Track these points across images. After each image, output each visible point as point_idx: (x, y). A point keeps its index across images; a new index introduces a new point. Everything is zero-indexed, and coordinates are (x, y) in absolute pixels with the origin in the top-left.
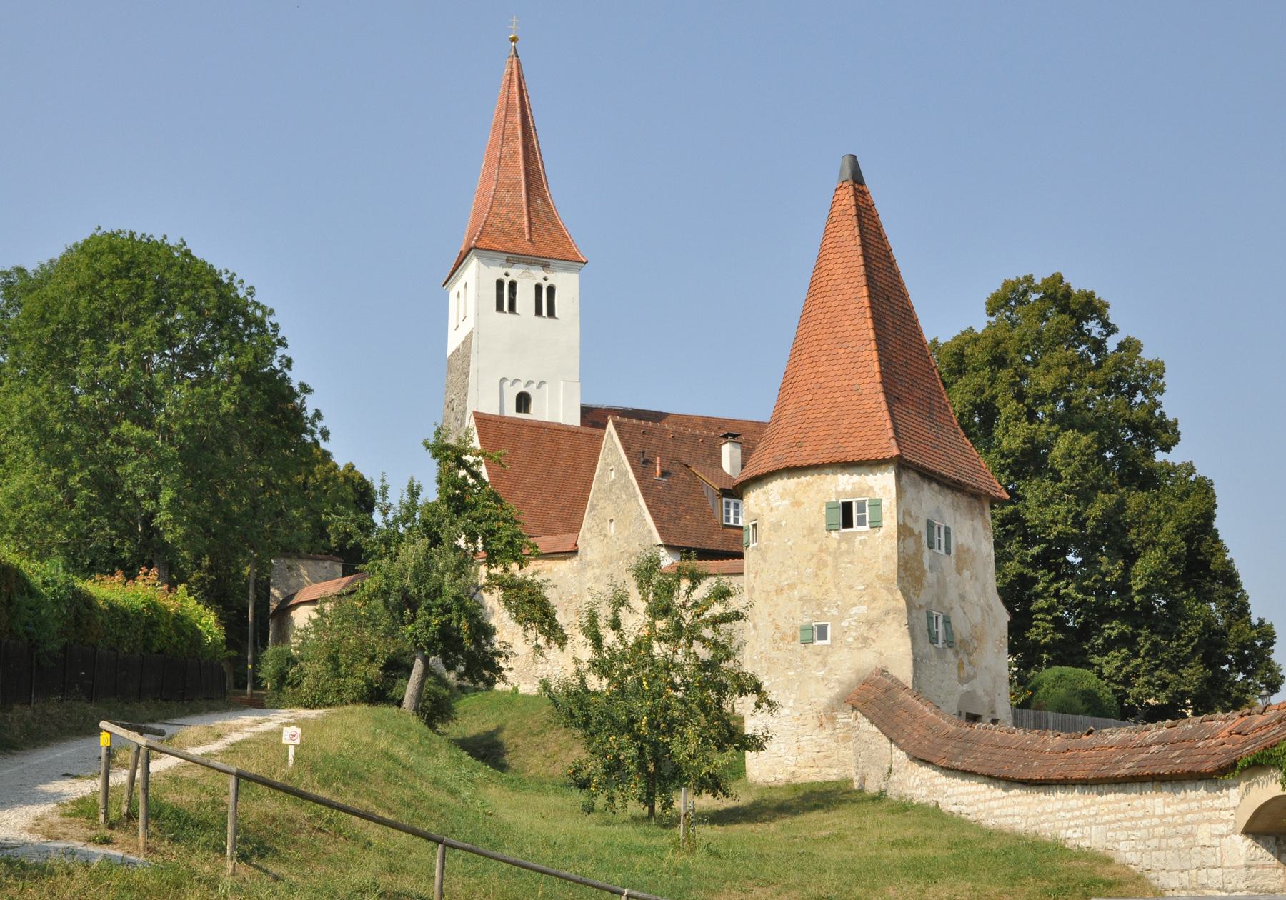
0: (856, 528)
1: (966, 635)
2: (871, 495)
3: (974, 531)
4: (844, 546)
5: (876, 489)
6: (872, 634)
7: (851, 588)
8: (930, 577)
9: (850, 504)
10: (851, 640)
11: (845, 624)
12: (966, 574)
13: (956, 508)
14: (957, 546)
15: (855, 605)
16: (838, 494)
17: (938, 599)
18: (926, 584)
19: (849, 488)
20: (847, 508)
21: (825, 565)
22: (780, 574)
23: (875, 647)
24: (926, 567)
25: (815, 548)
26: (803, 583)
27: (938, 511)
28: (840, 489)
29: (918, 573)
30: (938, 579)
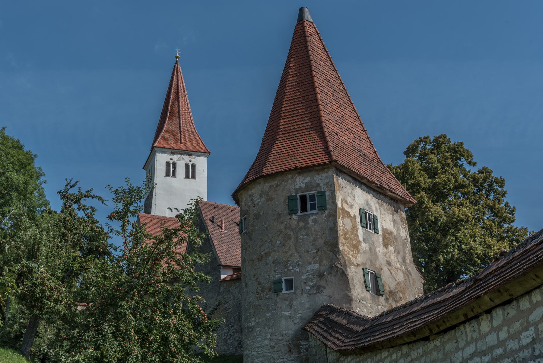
0: (310, 212)
1: (392, 288)
2: (318, 189)
3: (394, 222)
4: (301, 224)
5: (322, 185)
6: (322, 283)
7: (307, 252)
8: (364, 246)
9: (305, 196)
10: (308, 288)
11: (304, 277)
12: (391, 248)
13: (381, 205)
14: (383, 230)
15: (310, 263)
16: (297, 190)
17: (371, 261)
18: (361, 250)
19: (303, 186)
20: (303, 198)
21: (290, 238)
22: (260, 247)
23: (325, 292)
24: (361, 239)
25: (282, 226)
26: (275, 251)
27: (367, 203)
28: (298, 187)
29: (354, 242)
30: (370, 248)
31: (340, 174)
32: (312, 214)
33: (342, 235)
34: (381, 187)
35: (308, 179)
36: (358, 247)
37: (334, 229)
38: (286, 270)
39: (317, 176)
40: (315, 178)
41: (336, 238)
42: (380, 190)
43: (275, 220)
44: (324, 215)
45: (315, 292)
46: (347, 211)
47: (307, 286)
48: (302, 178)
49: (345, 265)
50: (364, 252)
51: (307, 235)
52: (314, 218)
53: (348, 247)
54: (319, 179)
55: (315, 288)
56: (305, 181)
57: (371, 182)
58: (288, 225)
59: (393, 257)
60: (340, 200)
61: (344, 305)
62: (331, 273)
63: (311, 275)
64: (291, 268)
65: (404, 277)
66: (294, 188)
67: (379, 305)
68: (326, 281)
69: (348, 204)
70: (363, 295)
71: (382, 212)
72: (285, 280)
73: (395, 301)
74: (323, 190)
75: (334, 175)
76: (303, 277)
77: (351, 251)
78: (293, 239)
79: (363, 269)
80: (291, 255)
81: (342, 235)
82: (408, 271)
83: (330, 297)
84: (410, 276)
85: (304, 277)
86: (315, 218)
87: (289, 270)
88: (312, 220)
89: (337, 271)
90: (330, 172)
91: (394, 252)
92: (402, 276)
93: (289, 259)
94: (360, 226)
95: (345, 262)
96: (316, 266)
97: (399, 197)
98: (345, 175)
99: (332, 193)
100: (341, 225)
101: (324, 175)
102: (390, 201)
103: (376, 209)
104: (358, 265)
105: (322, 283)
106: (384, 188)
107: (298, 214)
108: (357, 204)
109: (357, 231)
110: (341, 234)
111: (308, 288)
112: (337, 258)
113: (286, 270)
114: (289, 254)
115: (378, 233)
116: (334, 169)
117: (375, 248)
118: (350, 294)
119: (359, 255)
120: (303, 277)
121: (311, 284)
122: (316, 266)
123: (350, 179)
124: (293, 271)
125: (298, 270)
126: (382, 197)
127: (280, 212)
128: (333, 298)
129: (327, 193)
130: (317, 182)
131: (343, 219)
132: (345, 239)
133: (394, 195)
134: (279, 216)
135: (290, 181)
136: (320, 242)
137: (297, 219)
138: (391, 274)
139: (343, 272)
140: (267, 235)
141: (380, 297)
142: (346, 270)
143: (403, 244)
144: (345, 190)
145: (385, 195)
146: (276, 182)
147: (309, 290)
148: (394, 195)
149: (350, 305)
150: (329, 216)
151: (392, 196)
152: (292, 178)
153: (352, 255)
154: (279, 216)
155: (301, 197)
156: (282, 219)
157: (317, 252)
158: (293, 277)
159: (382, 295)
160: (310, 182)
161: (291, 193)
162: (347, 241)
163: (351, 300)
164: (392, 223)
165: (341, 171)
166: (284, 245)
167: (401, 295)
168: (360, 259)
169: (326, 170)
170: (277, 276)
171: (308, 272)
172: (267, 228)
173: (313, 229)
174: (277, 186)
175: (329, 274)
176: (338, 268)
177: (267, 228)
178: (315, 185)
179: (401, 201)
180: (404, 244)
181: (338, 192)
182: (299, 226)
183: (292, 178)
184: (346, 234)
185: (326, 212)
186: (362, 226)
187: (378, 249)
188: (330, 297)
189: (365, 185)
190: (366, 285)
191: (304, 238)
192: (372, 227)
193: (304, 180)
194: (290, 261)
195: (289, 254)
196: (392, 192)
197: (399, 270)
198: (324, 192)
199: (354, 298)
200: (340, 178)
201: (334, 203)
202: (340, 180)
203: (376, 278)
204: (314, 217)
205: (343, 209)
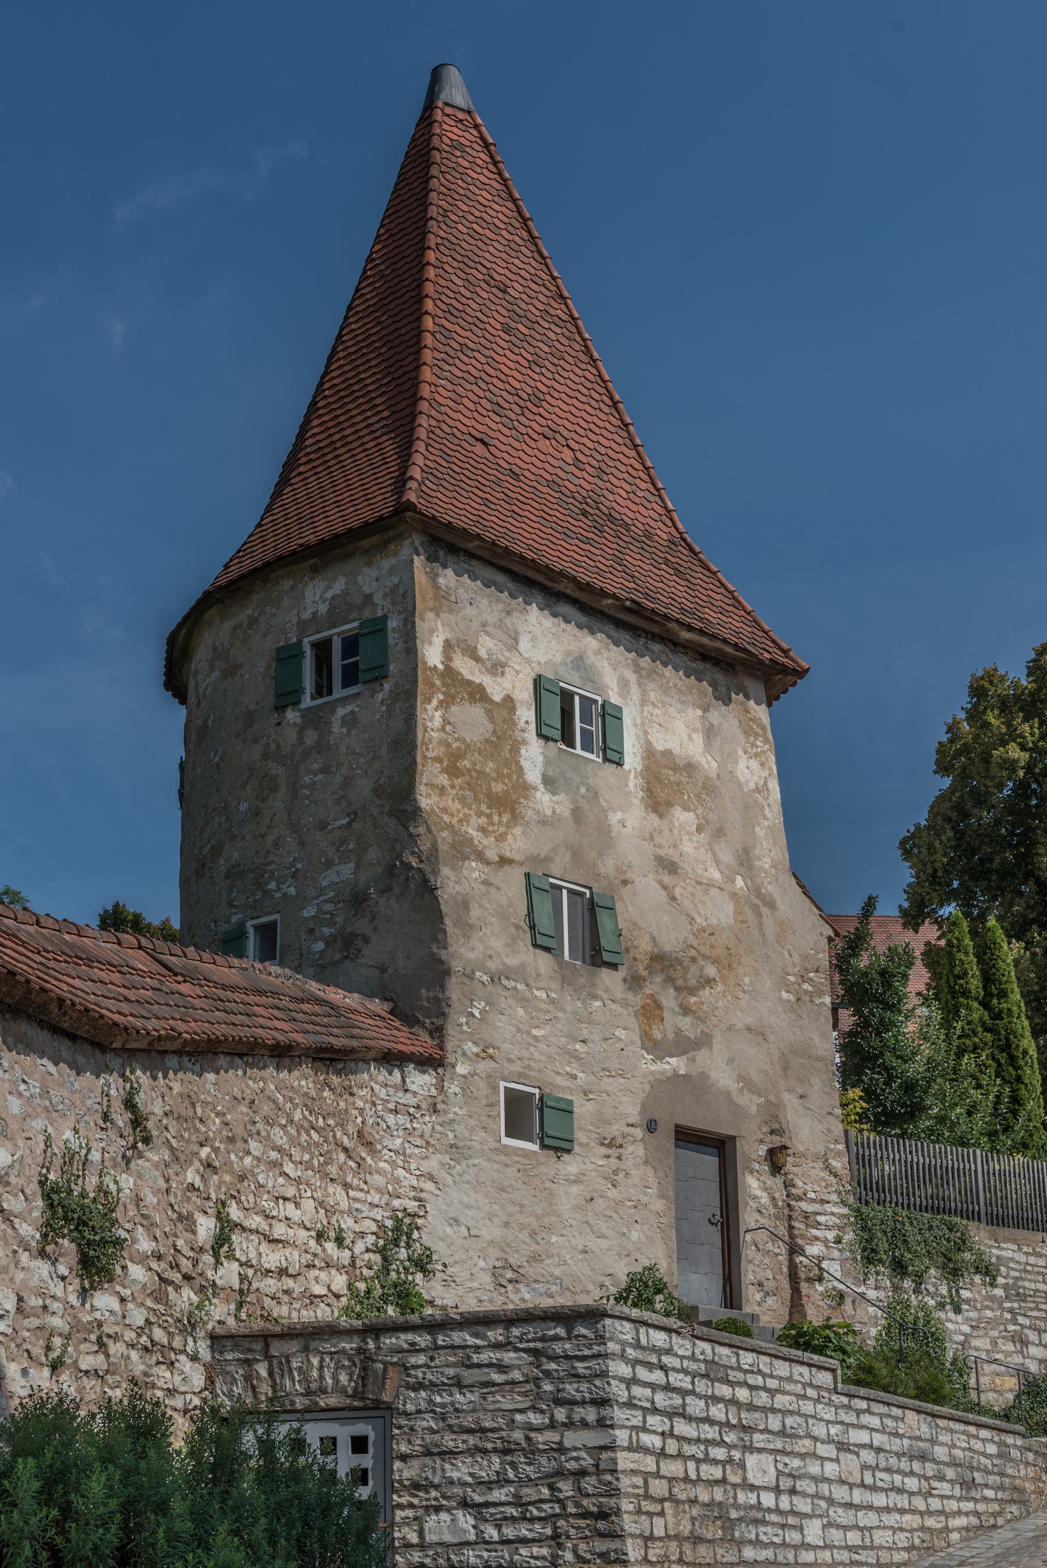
0: (338, 692)
2: (367, 614)
3: (710, 733)
4: (311, 737)
5: (378, 598)
6: (362, 925)
9: (328, 641)
10: (320, 946)
11: (309, 912)
14: (649, 753)
15: (329, 864)
16: (303, 627)
19: (323, 609)
21: (274, 789)
24: (533, 775)
26: (233, 838)
27: (579, 662)
28: (306, 615)
29: (498, 788)
30: (577, 814)
31: (450, 559)
32: (343, 701)
33: (438, 760)
34: (637, 609)
35: (339, 585)
36: (516, 802)
37: (404, 743)
38: (259, 896)
39: (367, 571)
40: (360, 580)
41: (410, 771)
42: (645, 624)
43: (237, 736)
44: (380, 697)
45: (338, 956)
46: (469, 683)
47: (317, 939)
48: (323, 584)
49: (433, 857)
50: (543, 822)
51: (325, 770)
52: (355, 711)
53: (462, 800)
54: (370, 578)
55: (339, 943)
56: (329, 595)
57: (603, 593)
58: (273, 747)
59: (691, 849)
60: (438, 641)
61: (423, 991)
62: (390, 889)
63: (329, 901)
64: (272, 885)
65: (738, 912)
66: (295, 620)
67: (595, 997)
68: (373, 919)
69: (477, 659)
70: (512, 961)
71: (653, 696)
72: (256, 928)
73: (677, 989)
74: (380, 614)
75: (418, 561)
76: (306, 913)
77: (480, 814)
78: (283, 789)
79: (527, 876)
80: (276, 844)
81: (438, 760)
82: (759, 895)
83: (383, 969)
84: (765, 910)
85: (309, 912)
86: (352, 712)
87: (267, 894)
88: (343, 717)
89: (407, 879)
90: (405, 551)
91: (700, 829)
92: (729, 908)
93: (271, 858)
94: (531, 734)
95: (435, 847)
96: (347, 870)
97: (729, 649)
98: (474, 562)
99: (406, 619)
100: (438, 722)
101: (386, 564)
102: (699, 665)
103: (624, 684)
104: (504, 861)
105: (362, 925)
106: (665, 616)
107: (303, 706)
108: (528, 661)
109: (515, 750)
110: (430, 754)
111: (320, 946)
112: (411, 835)
113: (259, 896)
114: (269, 840)
115: (620, 764)
116: (417, 539)
117: (605, 812)
118: (443, 955)
119: (518, 831)
120: (306, 913)
121: (327, 931)
122: (347, 870)
123: (501, 578)
124: (278, 895)
125: (292, 891)
126: (657, 647)
127: (253, 707)
128: (391, 970)
129: (392, 623)
130: (367, 589)
131: (444, 705)
132: (453, 771)
133: (705, 640)
134: (250, 718)
135: (286, 602)
136: (363, 787)
137: (299, 720)
138: (673, 899)
139: (425, 881)
140: (217, 790)
141: (605, 973)
142: (436, 872)
143: (747, 807)
144: (469, 611)
145: (675, 644)
146: (249, 612)
147: (322, 952)
148: (705, 640)
149: (443, 988)
150: (395, 697)
151: (702, 646)
152: (293, 588)
153: (483, 830)
154: (250, 718)
155: (315, 645)
156: (255, 727)
157: (349, 825)
158: (277, 917)
159: (614, 966)
160: (345, 593)
161: (287, 639)
162: (458, 782)
163: (447, 972)
164: (699, 739)
165: (453, 549)
166: (257, 814)
167: (711, 971)
168: (518, 843)
169: (392, 547)
170: (234, 919)
171: (322, 891)
172: (218, 766)
173: (343, 749)
174: (253, 621)
175: (382, 892)
176: (409, 867)
177: (218, 766)
178: (359, 602)
179: (742, 662)
180: (750, 807)
181: (430, 616)
182: (302, 743)
183: (293, 588)
184: (456, 756)
185: (387, 687)
186: (540, 735)
187: (615, 817)
188: (383, 969)
189: (574, 602)
190: (532, 927)
191: (314, 783)
192: (598, 742)
193: (328, 588)
194: (272, 862)
195: (269, 840)
196: (690, 628)
197: (714, 891)
198: (384, 618)
199: (457, 966)
200: (449, 572)
201: (411, 651)
202: (447, 578)
203: (592, 910)
204: (349, 708)
205: (449, 673)
